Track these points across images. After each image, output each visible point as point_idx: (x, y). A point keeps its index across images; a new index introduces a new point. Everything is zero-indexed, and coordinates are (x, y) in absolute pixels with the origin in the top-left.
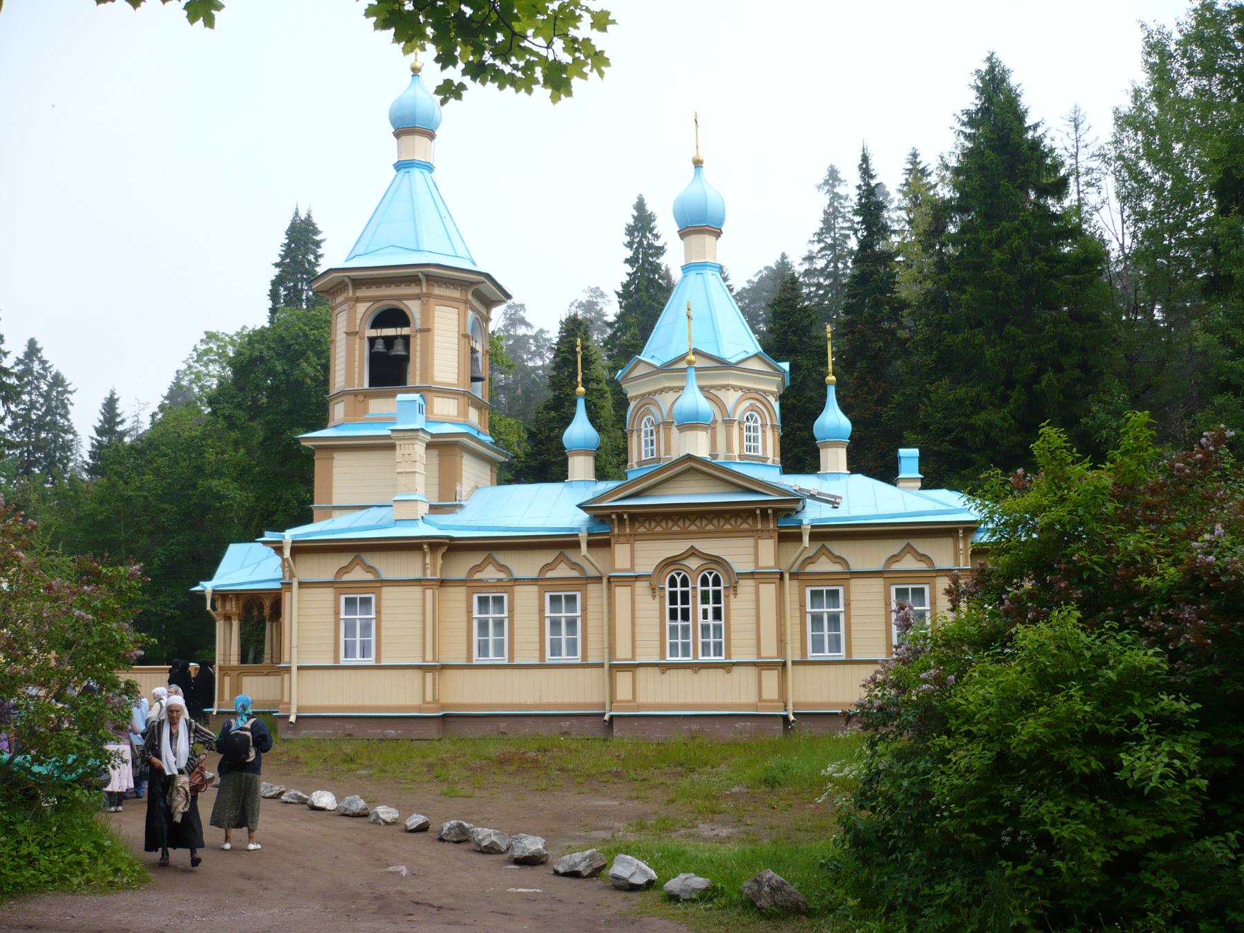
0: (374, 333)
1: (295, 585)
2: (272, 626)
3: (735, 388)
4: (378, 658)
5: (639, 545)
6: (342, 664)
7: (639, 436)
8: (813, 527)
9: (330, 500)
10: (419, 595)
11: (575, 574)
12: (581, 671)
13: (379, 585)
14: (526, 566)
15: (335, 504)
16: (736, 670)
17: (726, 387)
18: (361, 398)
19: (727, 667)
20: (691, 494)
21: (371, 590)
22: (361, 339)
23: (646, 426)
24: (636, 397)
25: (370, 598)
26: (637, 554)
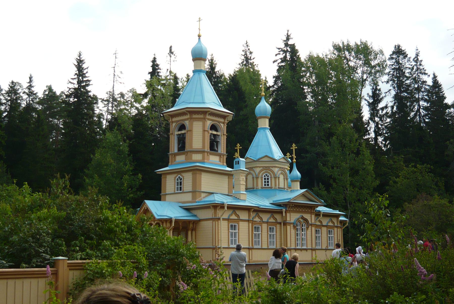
0: (211, 132)
1: (221, 219)
2: (192, 233)
3: (277, 167)
4: (262, 246)
5: (292, 214)
6: (230, 247)
7: (262, 180)
8: (323, 213)
9: (201, 190)
10: (248, 225)
11: (274, 221)
12: (267, 250)
14: (265, 217)
15: (202, 190)
16: (308, 251)
17: (275, 167)
18: (208, 154)
19: (306, 250)
20: (302, 201)
21: (236, 222)
22: (208, 133)
23: (265, 176)
24: (260, 167)
25: (231, 225)
26: (291, 216)
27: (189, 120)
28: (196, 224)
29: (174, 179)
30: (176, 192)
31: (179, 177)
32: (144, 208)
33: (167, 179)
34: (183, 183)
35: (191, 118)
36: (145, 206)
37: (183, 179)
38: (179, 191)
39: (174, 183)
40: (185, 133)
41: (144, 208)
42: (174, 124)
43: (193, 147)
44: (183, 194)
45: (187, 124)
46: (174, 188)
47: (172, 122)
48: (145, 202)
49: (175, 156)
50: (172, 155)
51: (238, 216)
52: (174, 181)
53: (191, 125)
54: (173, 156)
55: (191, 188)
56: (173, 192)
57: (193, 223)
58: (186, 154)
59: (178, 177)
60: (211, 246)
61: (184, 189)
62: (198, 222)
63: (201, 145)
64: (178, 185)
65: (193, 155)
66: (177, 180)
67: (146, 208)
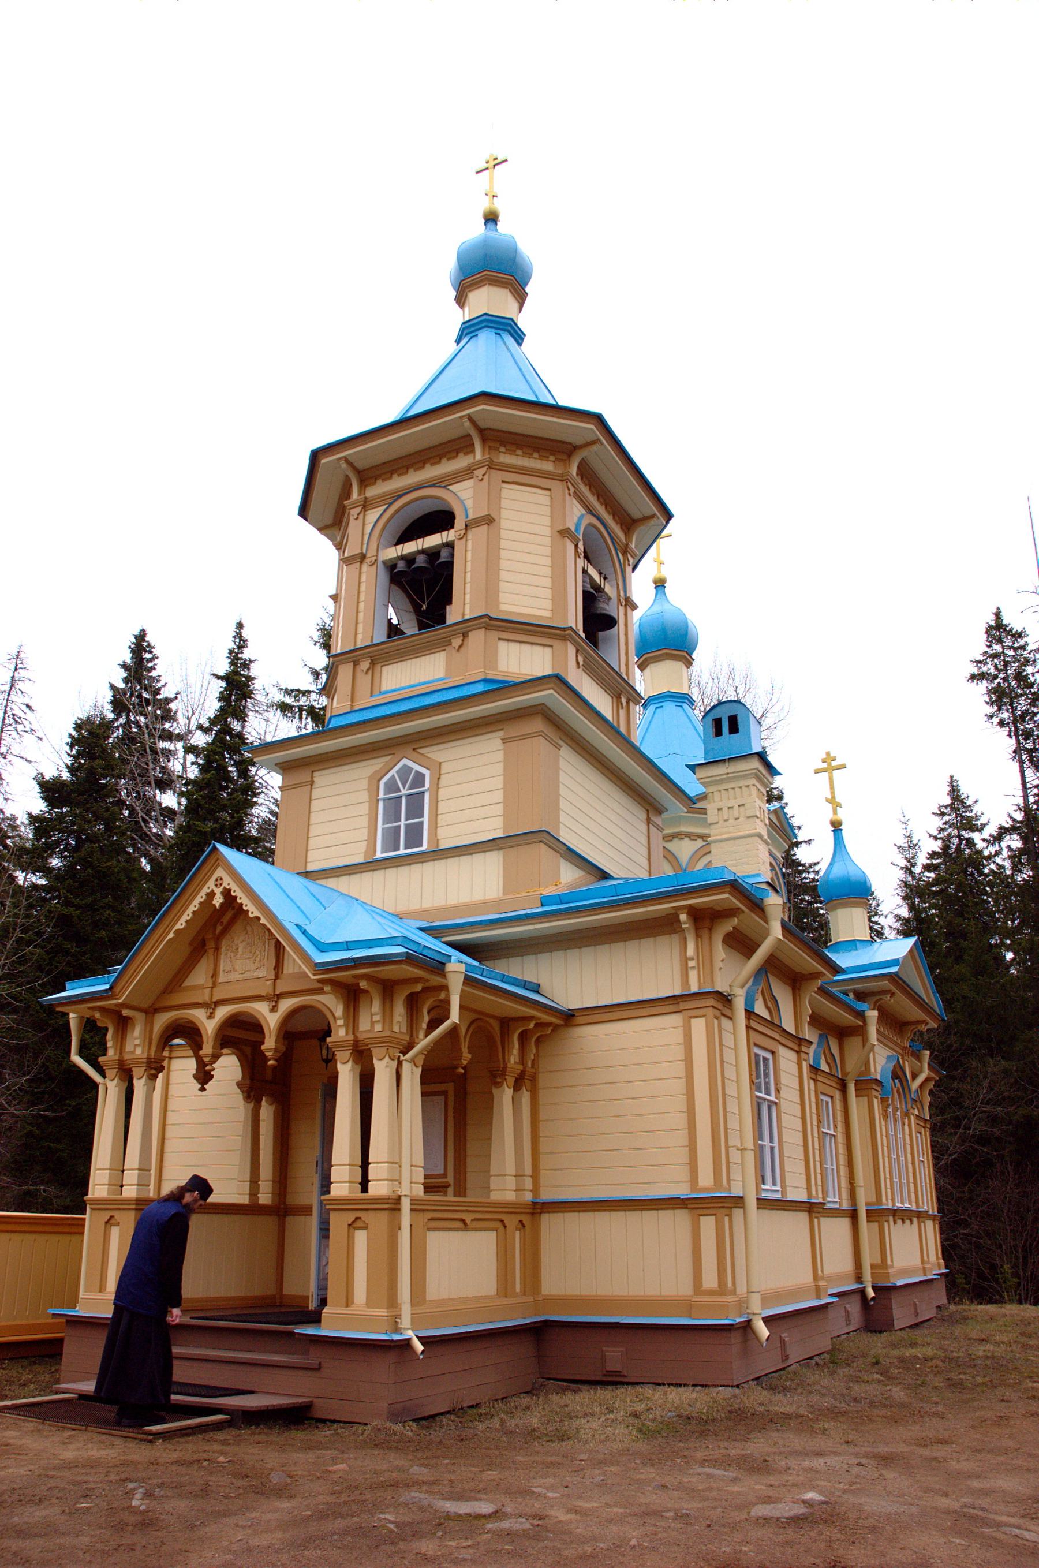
13: (777, 1036)
27: (479, 473)
28: (538, 1041)
29: (365, 784)
30: (379, 855)
31: (405, 771)
32: (205, 890)
33: (316, 793)
34: (435, 802)
35: (491, 466)
36: (211, 884)
37: (437, 779)
38: (402, 851)
39: (365, 809)
40: (450, 545)
41: (201, 897)
42: (373, 515)
43: (503, 607)
44: (428, 867)
45: (463, 495)
46: (364, 834)
47: (366, 505)
48: (215, 848)
49: (373, 663)
50: (356, 663)
51: (773, 1004)
52: (365, 796)
53: (494, 498)
54: (365, 665)
55: (499, 822)
56: (360, 859)
57: (524, 1037)
58: (456, 642)
59: (393, 772)
60: (682, 1191)
61: (442, 833)
62: (556, 1028)
63: (548, 604)
64: (393, 814)
65: (503, 646)
66: (391, 787)
67: (218, 900)
